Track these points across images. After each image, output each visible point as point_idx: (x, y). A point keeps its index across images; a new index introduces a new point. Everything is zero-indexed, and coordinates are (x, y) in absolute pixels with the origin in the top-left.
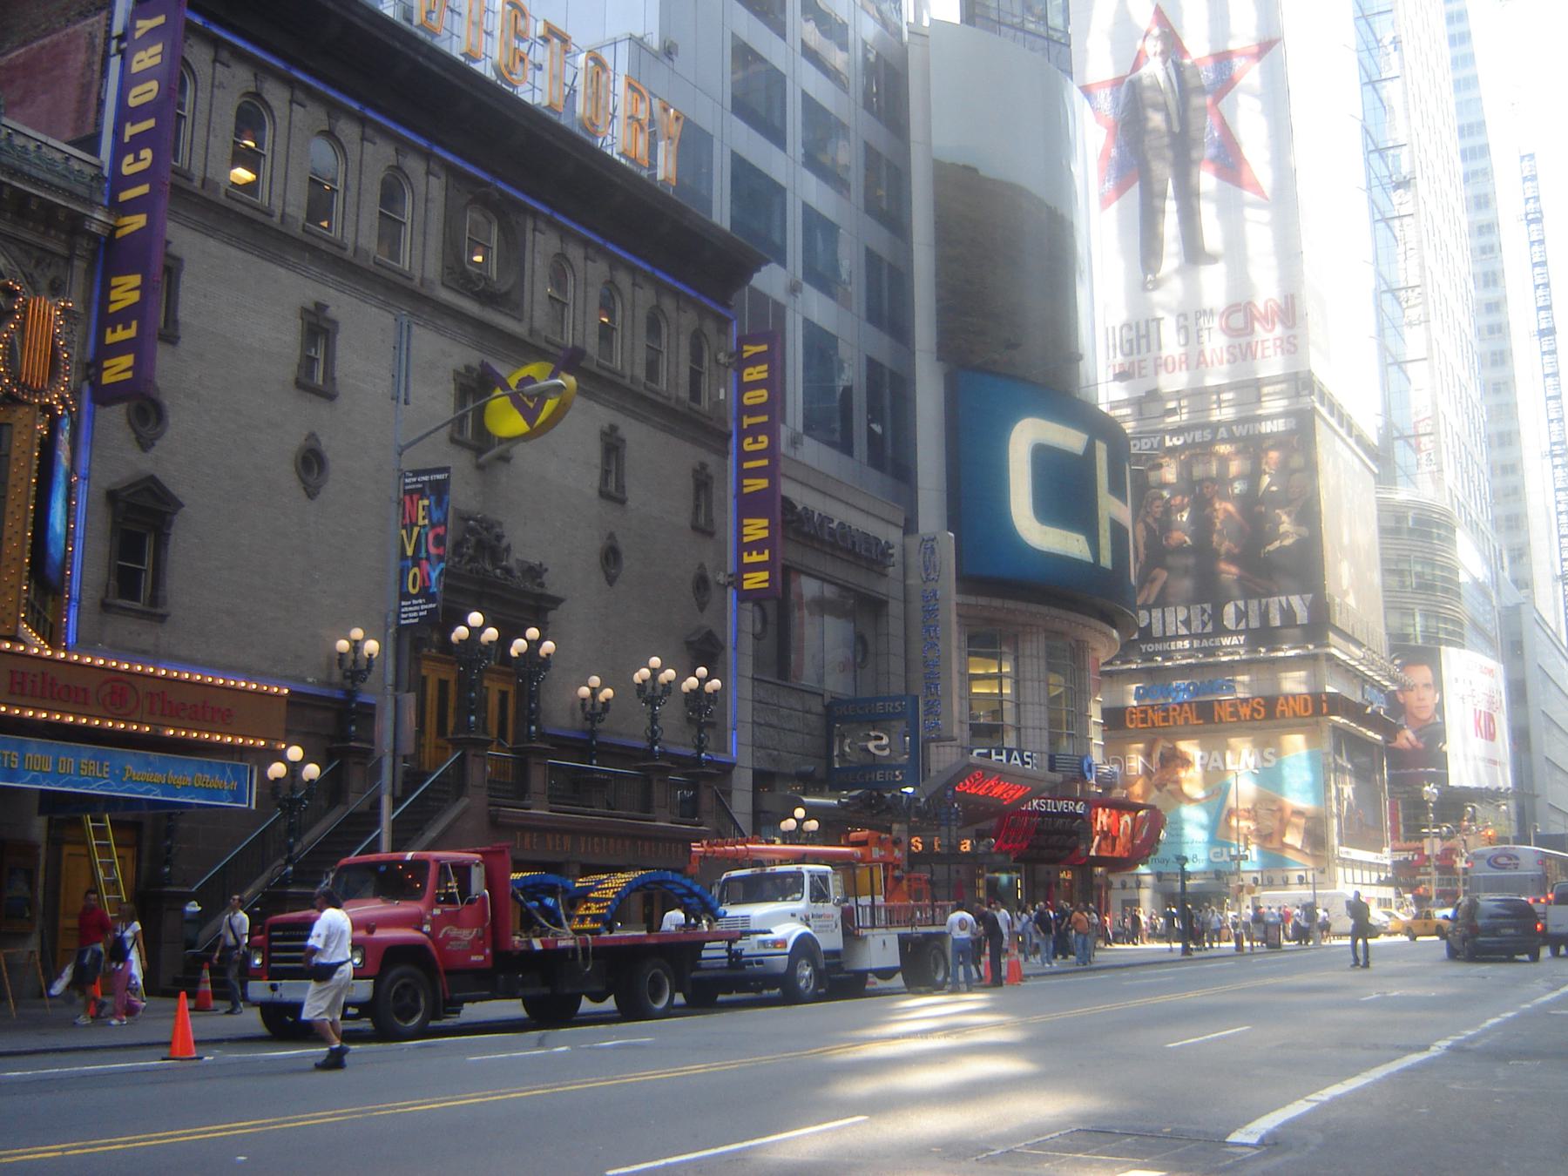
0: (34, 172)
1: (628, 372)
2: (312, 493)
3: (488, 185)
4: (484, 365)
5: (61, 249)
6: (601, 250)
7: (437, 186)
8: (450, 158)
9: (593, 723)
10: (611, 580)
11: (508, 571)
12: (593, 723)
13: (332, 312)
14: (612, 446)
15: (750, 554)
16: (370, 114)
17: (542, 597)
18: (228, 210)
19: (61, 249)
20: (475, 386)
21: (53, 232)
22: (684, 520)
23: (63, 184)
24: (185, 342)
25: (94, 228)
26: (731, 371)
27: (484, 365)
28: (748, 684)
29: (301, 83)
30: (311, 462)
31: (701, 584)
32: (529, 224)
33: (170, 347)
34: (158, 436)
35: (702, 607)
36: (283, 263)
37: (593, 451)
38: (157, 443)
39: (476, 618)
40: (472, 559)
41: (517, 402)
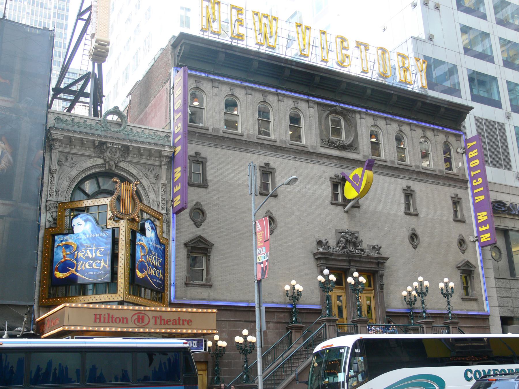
0: (142, 140)
1: (413, 164)
3: (335, 106)
4: (342, 173)
5: (158, 163)
6: (391, 120)
7: (314, 111)
8: (317, 100)
9: (411, 305)
10: (415, 247)
11: (362, 250)
12: (411, 305)
13: (272, 165)
14: (409, 194)
15: (482, 227)
16: (279, 91)
17: (377, 258)
18: (224, 137)
19: (158, 163)
20: (338, 183)
21: (153, 158)
23: (153, 141)
24: (210, 187)
25: (166, 154)
26: (464, 155)
27: (342, 173)
28: (493, 280)
29: (249, 87)
31: (461, 242)
32: (358, 116)
33: (205, 189)
34: (203, 221)
36: (249, 152)
38: (202, 224)
40: (344, 248)
41: (353, 185)
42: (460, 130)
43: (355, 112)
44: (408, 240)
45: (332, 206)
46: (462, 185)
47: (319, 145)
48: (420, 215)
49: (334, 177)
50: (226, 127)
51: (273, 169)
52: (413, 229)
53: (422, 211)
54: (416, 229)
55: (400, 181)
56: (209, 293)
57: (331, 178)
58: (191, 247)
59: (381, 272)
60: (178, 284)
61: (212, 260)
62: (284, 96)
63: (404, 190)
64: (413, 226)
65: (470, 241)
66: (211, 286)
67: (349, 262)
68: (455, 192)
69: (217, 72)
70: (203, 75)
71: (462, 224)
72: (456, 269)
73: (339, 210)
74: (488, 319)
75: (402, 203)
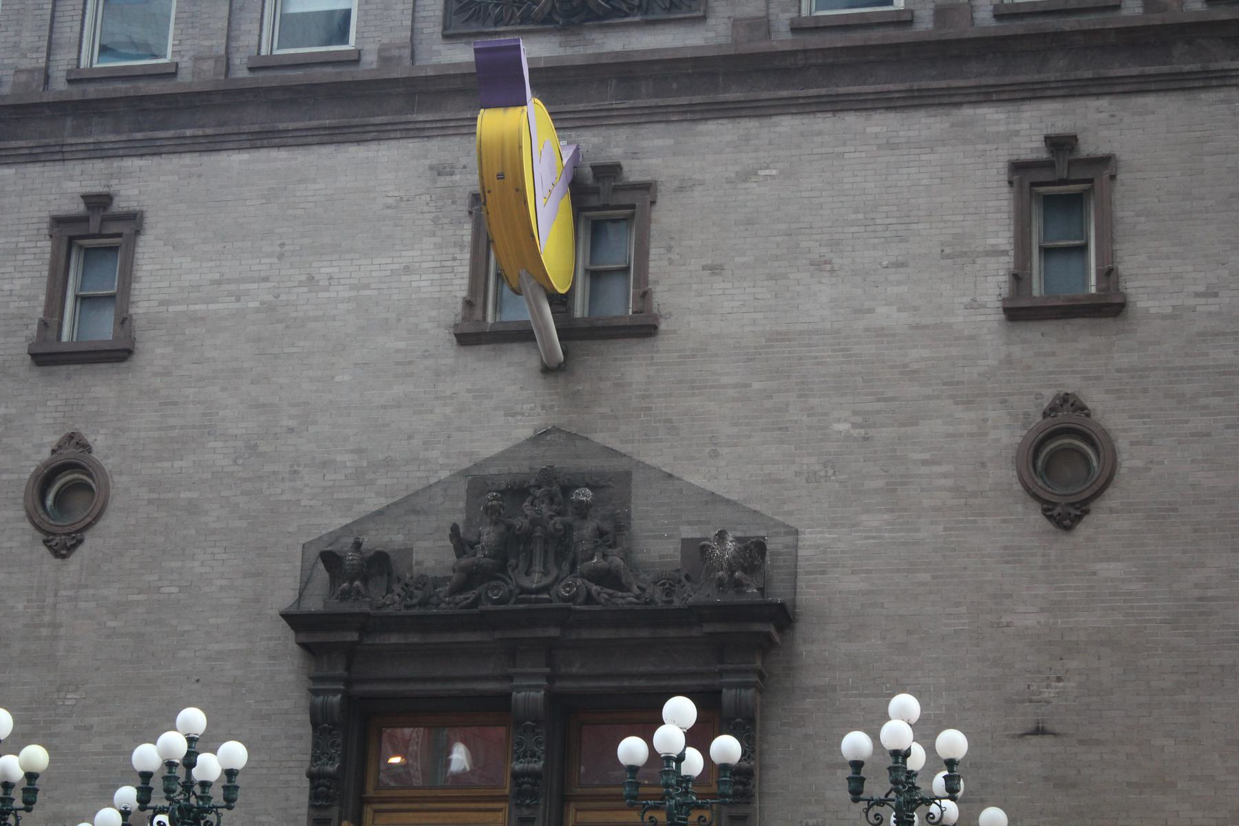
2: (62, 545)
10: (1065, 516)
11: (609, 578)
14: (1061, 190)
44: (1007, 475)
47: (432, 27)
51: (134, 219)
52: (1067, 402)
53: (1148, 279)
54: (1095, 399)
55: (992, 117)
59: (728, 695)
63: (1018, 168)
64: (1071, 384)
75: (996, 252)
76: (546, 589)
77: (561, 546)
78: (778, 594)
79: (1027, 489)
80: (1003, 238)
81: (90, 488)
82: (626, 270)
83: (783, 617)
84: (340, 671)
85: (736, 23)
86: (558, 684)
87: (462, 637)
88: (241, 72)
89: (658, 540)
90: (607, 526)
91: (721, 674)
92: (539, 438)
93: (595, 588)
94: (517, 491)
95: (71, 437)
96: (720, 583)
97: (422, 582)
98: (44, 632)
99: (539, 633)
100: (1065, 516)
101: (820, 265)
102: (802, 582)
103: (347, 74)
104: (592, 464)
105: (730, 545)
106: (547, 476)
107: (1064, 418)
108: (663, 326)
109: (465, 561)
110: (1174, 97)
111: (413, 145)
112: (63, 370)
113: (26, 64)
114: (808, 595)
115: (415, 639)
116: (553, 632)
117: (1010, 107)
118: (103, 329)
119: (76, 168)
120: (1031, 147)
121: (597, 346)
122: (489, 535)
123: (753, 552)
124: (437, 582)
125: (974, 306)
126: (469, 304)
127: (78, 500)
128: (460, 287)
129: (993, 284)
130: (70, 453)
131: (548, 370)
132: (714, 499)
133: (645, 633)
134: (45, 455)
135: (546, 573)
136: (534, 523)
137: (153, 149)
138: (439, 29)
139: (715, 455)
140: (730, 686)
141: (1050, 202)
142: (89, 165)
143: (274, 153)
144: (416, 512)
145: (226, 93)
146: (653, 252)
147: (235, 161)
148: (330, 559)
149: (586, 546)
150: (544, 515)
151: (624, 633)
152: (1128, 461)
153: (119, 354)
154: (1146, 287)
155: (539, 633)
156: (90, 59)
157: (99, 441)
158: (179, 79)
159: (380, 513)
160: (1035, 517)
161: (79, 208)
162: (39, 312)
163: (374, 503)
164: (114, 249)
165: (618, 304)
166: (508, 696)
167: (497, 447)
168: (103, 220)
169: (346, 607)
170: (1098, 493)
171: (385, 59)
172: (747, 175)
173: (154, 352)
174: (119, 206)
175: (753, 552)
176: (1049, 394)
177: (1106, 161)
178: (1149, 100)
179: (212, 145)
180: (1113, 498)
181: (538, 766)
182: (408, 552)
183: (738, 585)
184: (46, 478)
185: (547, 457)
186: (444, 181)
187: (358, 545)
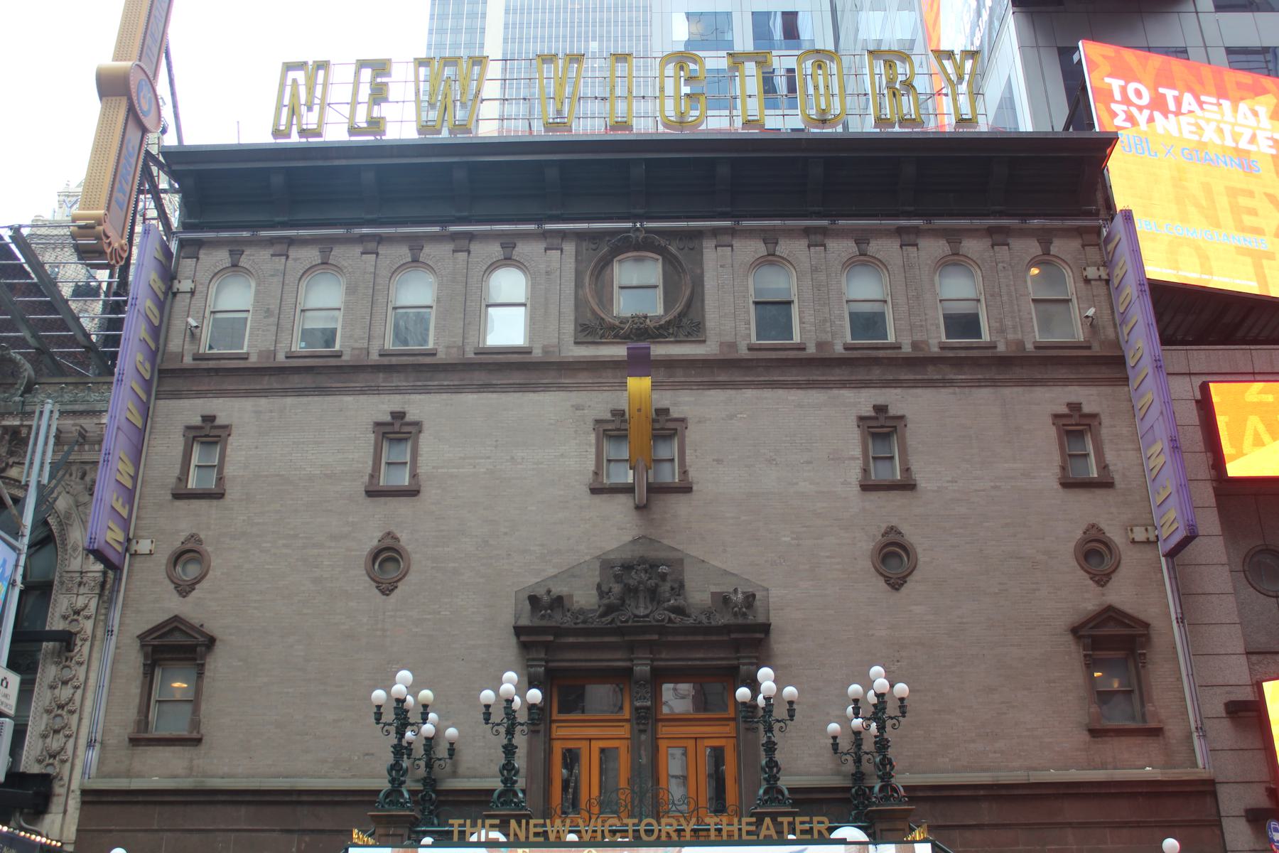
2: (387, 589)
3: (627, 230)
8: (571, 226)
10: (896, 584)
11: (680, 611)
14: (881, 429)
22: (1049, 475)
24: (233, 492)
30: (387, 561)
31: (1095, 554)
33: (215, 502)
34: (198, 580)
35: (1102, 579)
37: (852, 443)
39: (405, 675)
42: (1089, 214)
43: (698, 234)
45: (595, 497)
46: (1106, 372)
48: (922, 484)
49: (608, 416)
50: (303, 344)
51: (418, 424)
52: (892, 530)
54: (905, 528)
55: (848, 394)
56: (191, 760)
57: (598, 422)
58: (154, 646)
59: (743, 668)
60: (112, 741)
61: (207, 673)
62: (471, 237)
64: (894, 522)
65: (1133, 542)
66: (197, 741)
67: (631, 647)
68: (1073, 399)
69: (277, 219)
70: (245, 234)
71: (1110, 491)
72: (1070, 637)
73: (620, 508)
74: (1214, 795)
75: (853, 458)
76: (647, 616)
77: (653, 594)
78: (761, 619)
79: (877, 570)
80: (857, 452)
81: (397, 561)
82: (672, 460)
83: (766, 628)
84: (543, 656)
85: (722, 344)
86: (656, 663)
87: (607, 639)
88: (470, 355)
89: (699, 594)
90: (676, 586)
91: (738, 659)
92: (634, 541)
93: (673, 616)
94: (627, 567)
95: (389, 534)
96: (735, 614)
97: (582, 611)
98: (379, 633)
99: (648, 637)
100: (896, 584)
101: (770, 461)
102: (771, 615)
103: (526, 358)
104: (662, 555)
105: (740, 596)
106: (643, 560)
107: (892, 538)
108: (695, 488)
109: (606, 601)
110: (929, 390)
111: (562, 394)
112: (383, 499)
113: (357, 345)
114: (774, 620)
115: (581, 640)
116: (655, 637)
117: (855, 390)
118: (403, 479)
119: (386, 398)
120: (868, 411)
121: (662, 496)
122: (617, 588)
123: (750, 598)
124: (593, 611)
125: (845, 483)
126: (596, 474)
127: (390, 566)
128: (591, 466)
129: (854, 473)
130: (389, 543)
131: (638, 508)
132: (726, 573)
133: (700, 638)
134: (375, 543)
135: (646, 608)
136: (639, 583)
137: (426, 390)
138: (572, 339)
139: (725, 551)
140: (744, 664)
141: (875, 436)
142: (392, 397)
143: (490, 395)
144: (574, 576)
145: (464, 364)
146: (688, 452)
147: (470, 398)
148: (533, 600)
149: (667, 595)
150: (642, 579)
151: (690, 638)
152: (923, 558)
153: (412, 492)
154: (922, 475)
155: (648, 637)
156: (389, 345)
157: (405, 538)
158: (344, 358)
159: (555, 576)
160: (881, 583)
161: (388, 418)
162: (369, 470)
163: (552, 571)
164: (406, 439)
165: (669, 475)
166: (630, 670)
167: (614, 545)
168: (402, 425)
169: (544, 623)
170: (910, 573)
171: (546, 351)
172: (731, 417)
173: (430, 492)
174: (409, 418)
175: (750, 598)
176: (884, 527)
177: (902, 418)
178: (919, 391)
179: (458, 389)
180: (917, 575)
181: (649, 703)
182: (571, 596)
183: (744, 615)
184: (375, 555)
185: (639, 551)
186: (579, 413)
187: (549, 592)
